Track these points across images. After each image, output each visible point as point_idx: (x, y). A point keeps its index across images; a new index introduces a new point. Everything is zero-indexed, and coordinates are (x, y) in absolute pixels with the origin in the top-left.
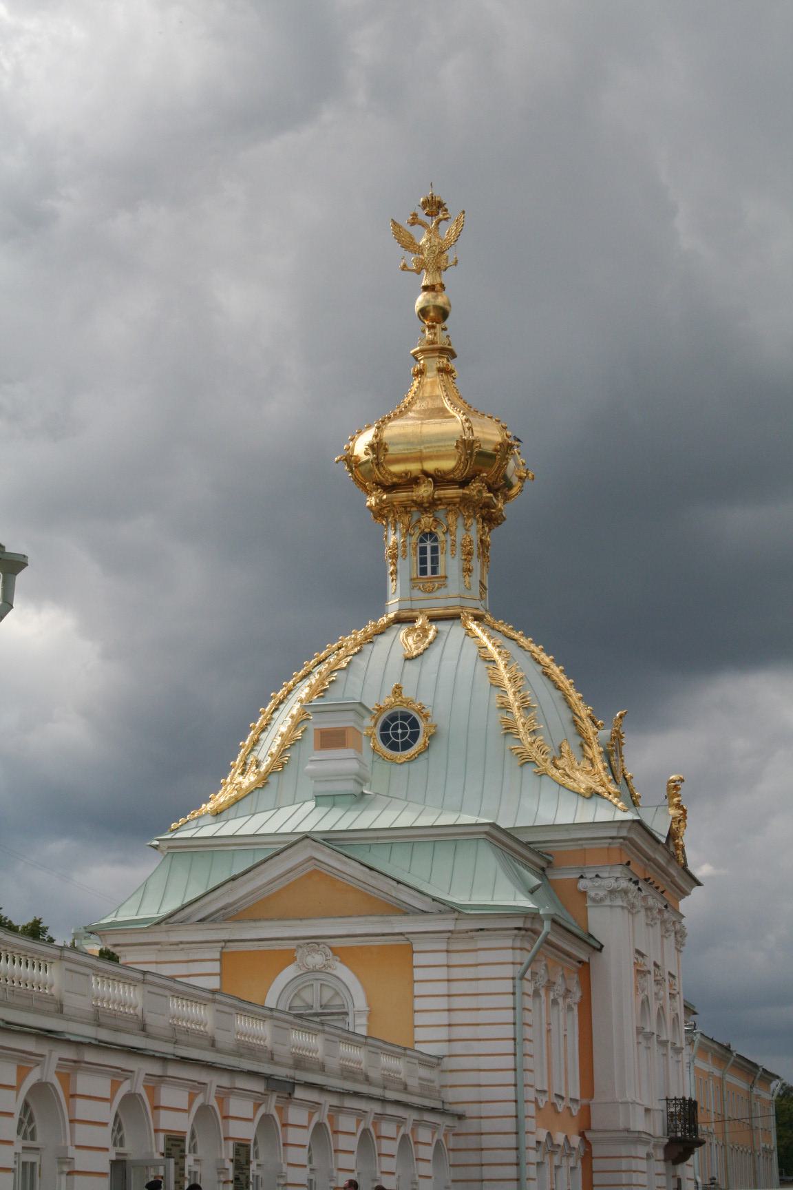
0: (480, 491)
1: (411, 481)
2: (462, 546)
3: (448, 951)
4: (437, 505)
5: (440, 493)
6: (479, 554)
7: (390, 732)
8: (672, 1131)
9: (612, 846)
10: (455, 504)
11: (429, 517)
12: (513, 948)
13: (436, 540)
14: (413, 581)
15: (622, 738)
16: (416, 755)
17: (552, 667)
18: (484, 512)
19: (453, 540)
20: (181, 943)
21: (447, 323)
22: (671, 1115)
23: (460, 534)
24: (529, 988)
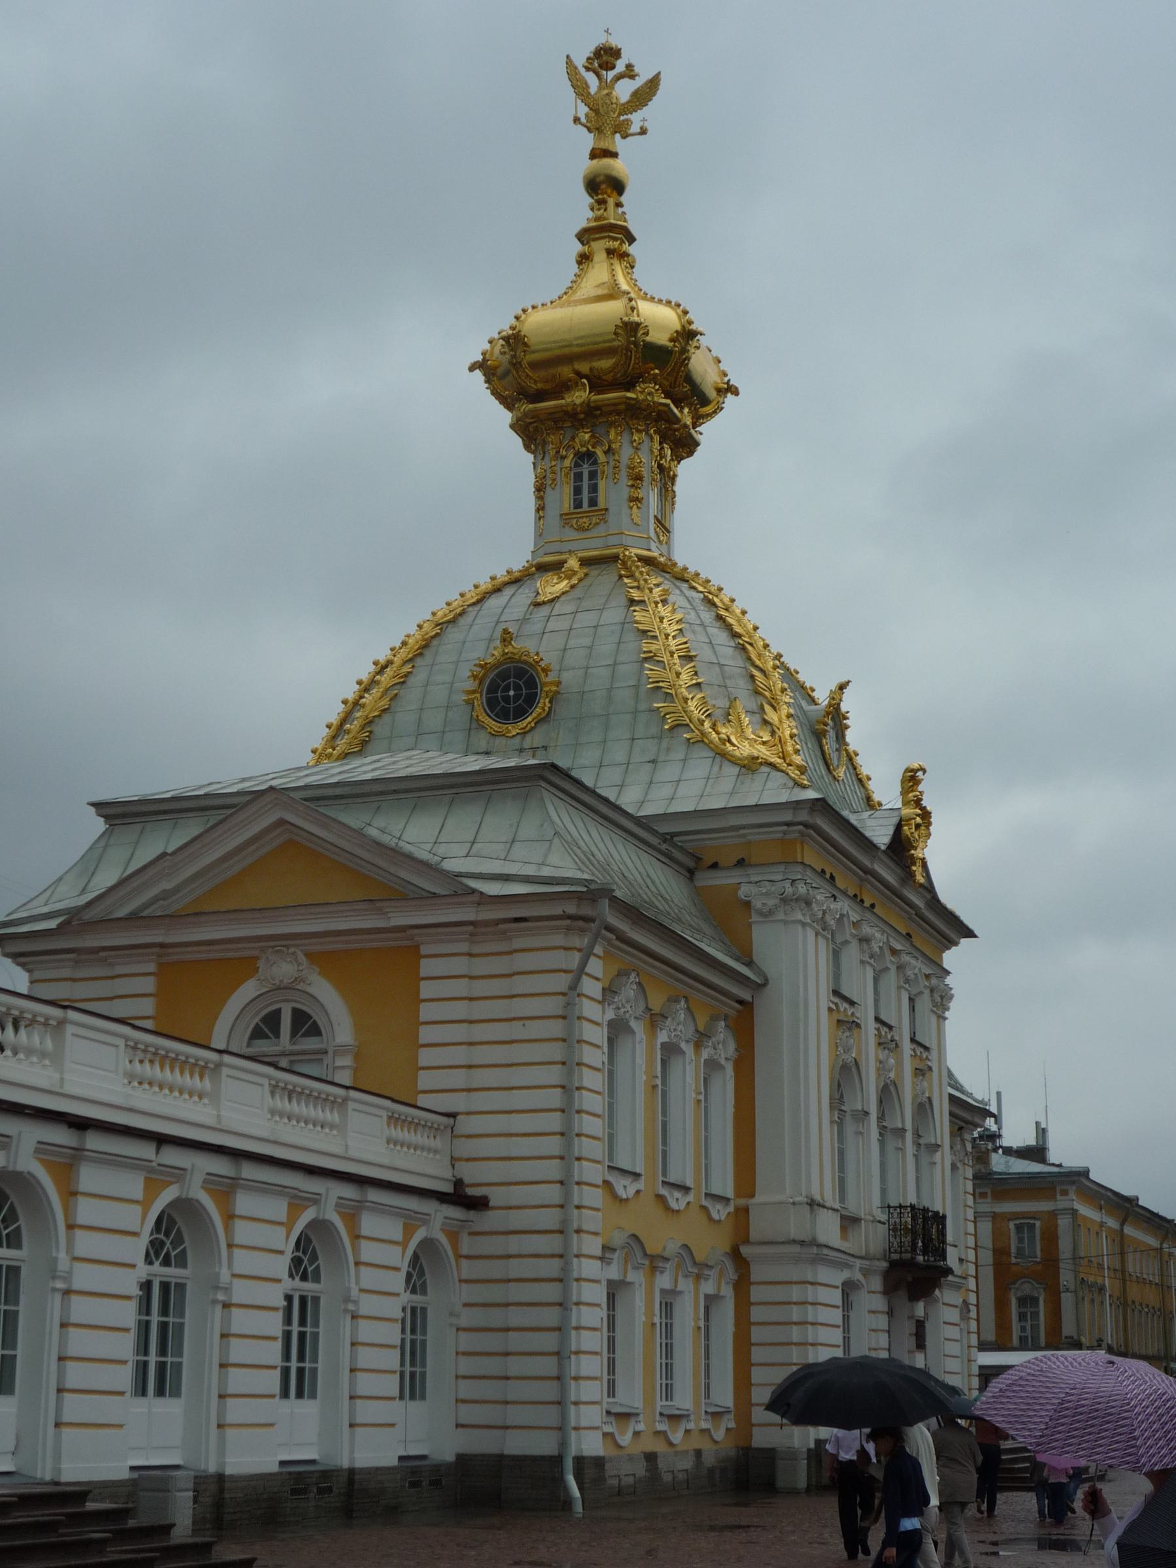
2: (629, 468)
4: (596, 417)
7: (499, 694)
8: (896, 1252)
9: (788, 837)
11: (586, 433)
13: (595, 463)
14: (564, 517)
16: (533, 725)
20: (104, 949)
22: (894, 1229)
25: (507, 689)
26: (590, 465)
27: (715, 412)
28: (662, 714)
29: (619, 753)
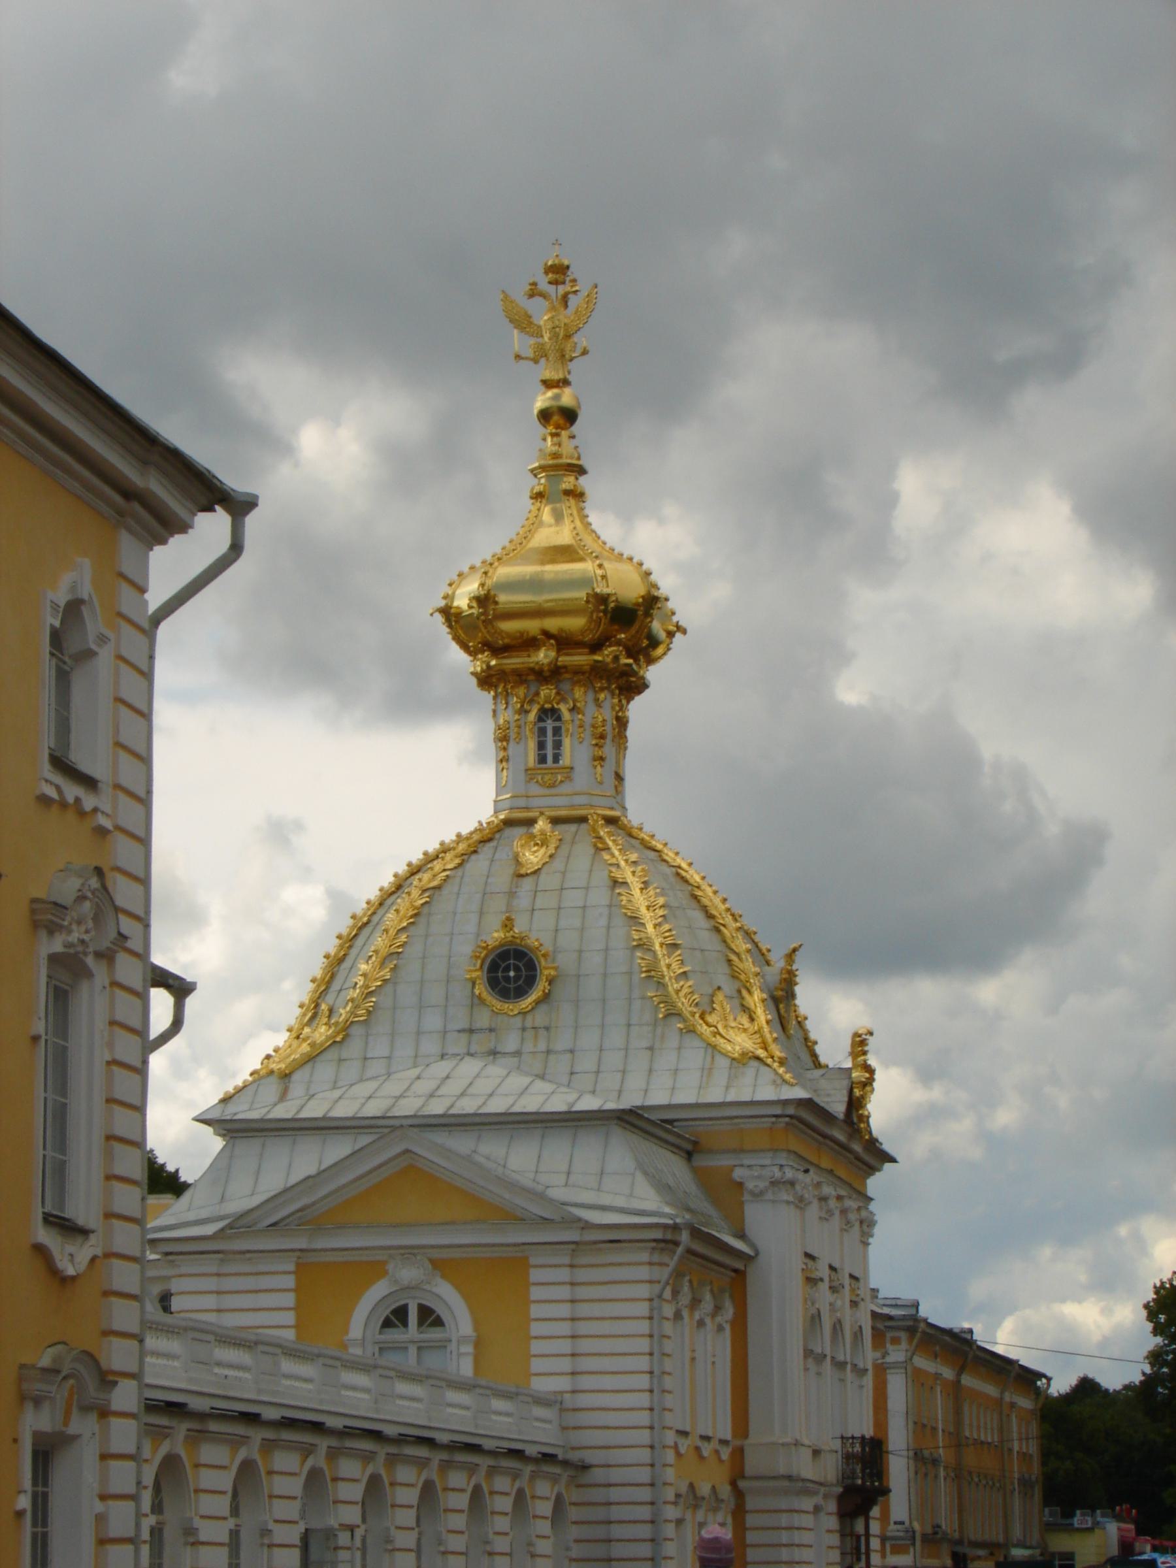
0: (616, 658)
1: (529, 643)
3: (572, 1266)
5: (564, 660)
6: (614, 736)
10: (583, 673)
12: (650, 1264)
13: (559, 719)
14: (529, 772)
15: (795, 976)
17: (703, 887)
18: (622, 681)
19: (581, 720)
20: (249, 1252)
21: (575, 429)
22: (848, 1457)
23: (591, 710)
24: (668, 1310)
25: (507, 969)
26: (554, 721)
27: (665, 654)
28: (656, 1003)
29: (616, 1038)
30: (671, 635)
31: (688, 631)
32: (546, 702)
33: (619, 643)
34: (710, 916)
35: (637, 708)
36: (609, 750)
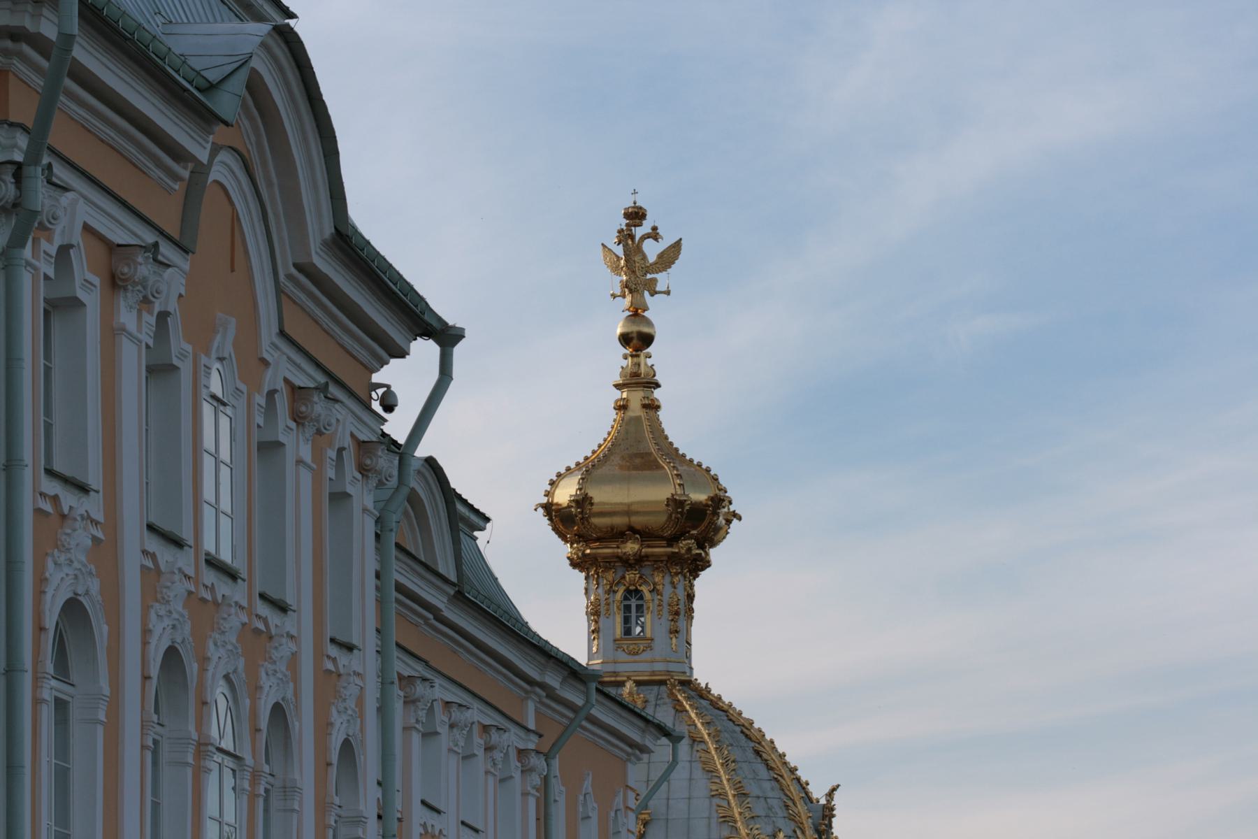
0: (689, 549)
2: (669, 605)
10: (662, 561)
13: (641, 598)
14: (617, 642)
19: (660, 600)
26: (637, 599)
30: (729, 522)
31: (743, 518)
32: (630, 585)
33: (691, 537)
34: (770, 768)
35: (702, 583)
36: (682, 623)
